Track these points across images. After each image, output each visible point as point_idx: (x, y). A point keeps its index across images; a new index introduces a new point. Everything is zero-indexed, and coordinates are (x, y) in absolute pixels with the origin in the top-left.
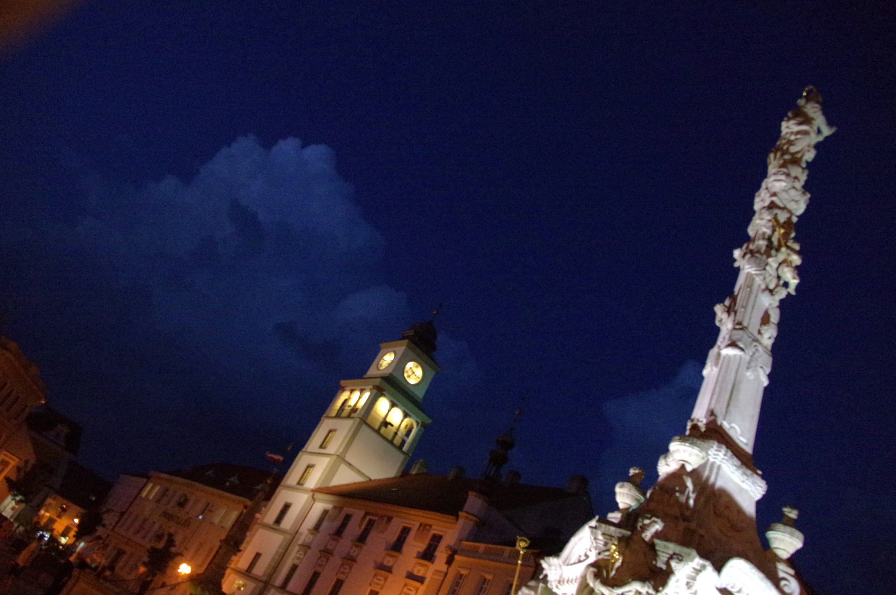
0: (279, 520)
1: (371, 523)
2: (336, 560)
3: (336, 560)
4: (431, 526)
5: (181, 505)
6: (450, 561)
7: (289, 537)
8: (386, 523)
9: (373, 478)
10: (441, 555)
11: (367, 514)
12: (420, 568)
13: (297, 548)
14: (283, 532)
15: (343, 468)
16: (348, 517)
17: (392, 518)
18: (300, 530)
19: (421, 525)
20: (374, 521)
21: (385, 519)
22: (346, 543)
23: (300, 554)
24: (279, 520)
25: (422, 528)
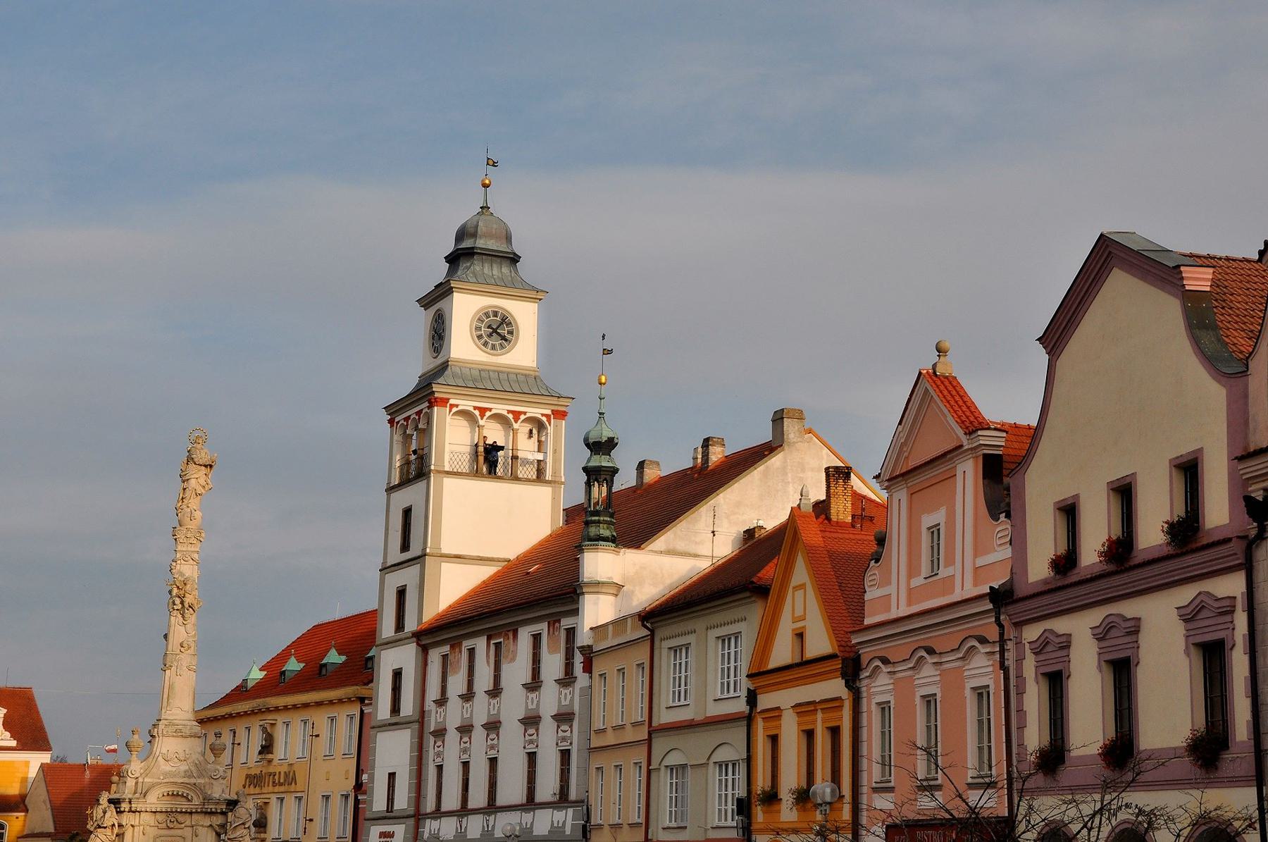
0: (395, 709)
1: (498, 645)
2: (479, 734)
3: (479, 734)
4: (559, 621)
5: (267, 748)
6: (588, 668)
7: (416, 726)
8: (514, 641)
9: (512, 555)
10: (578, 659)
11: (489, 638)
12: (566, 691)
13: (432, 739)
14: (405, 724)
15: (447, 568)
16: (472, 652)
17: (517, 629)
18: (427, 708)
19: (548, 624)
20: (501, 642)
21: (511, 637)
22: (481, 697)
23: (438, 747)
24: (395, 709)
25: (551, 630)
